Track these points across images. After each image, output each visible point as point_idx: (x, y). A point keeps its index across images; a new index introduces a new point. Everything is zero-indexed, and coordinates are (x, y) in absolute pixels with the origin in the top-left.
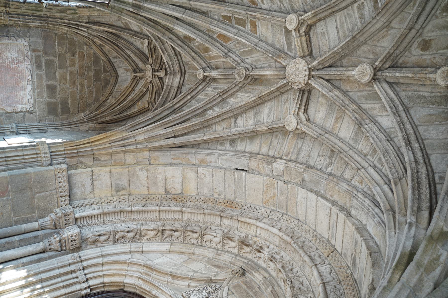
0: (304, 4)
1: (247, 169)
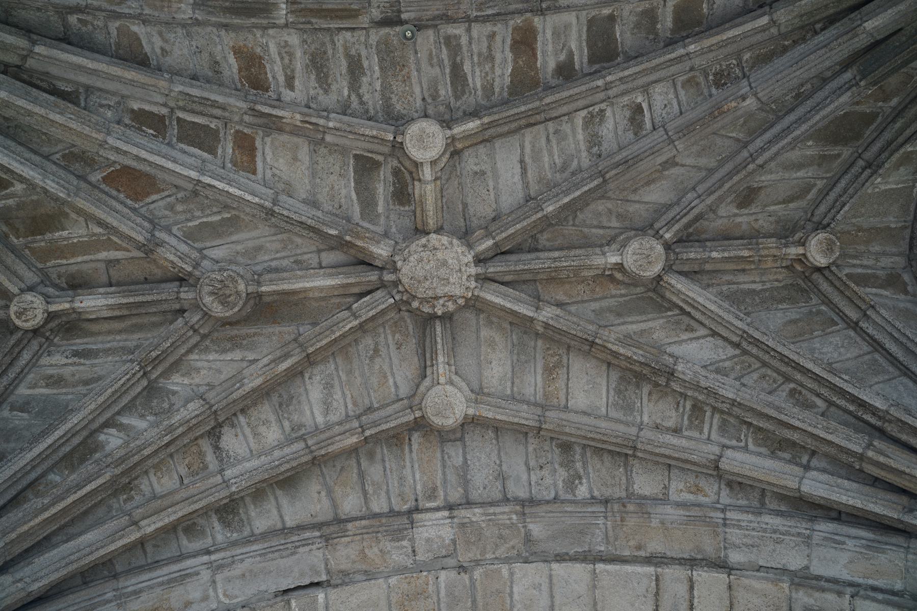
0: (429, 101)
1: (324, 578)
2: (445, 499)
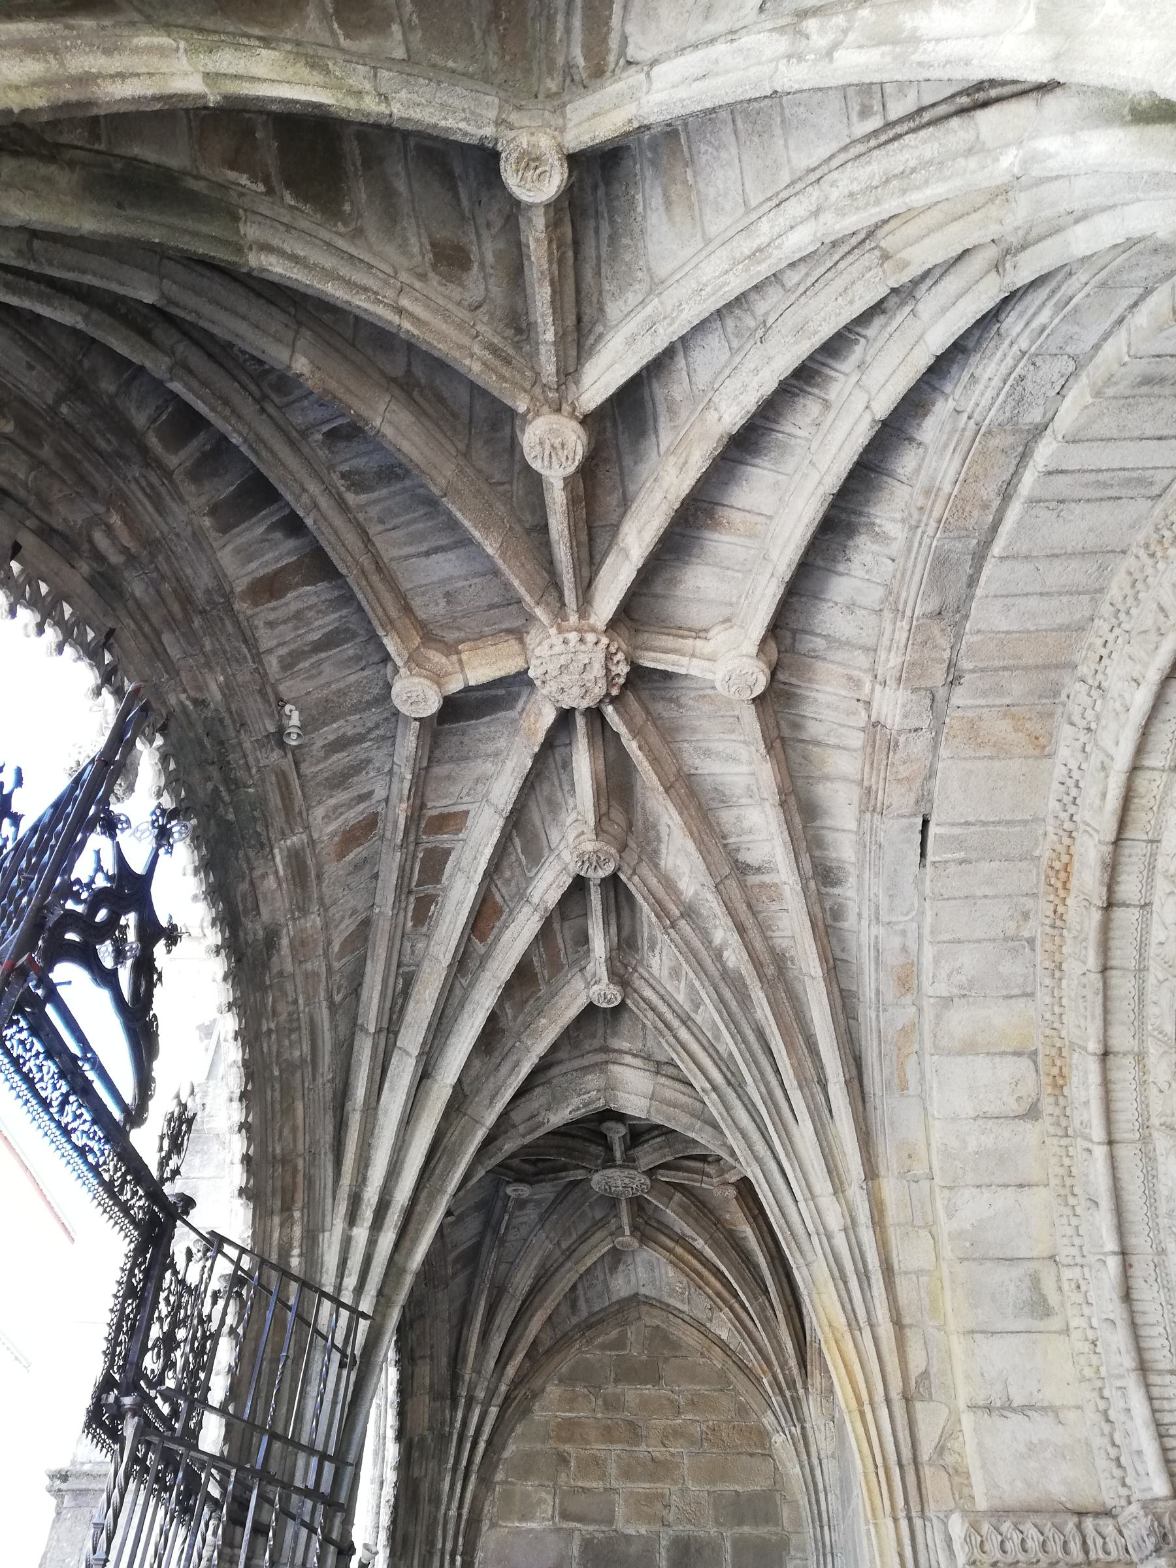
0: (363, 663)
1: (920, 820)
2: (865, 671)
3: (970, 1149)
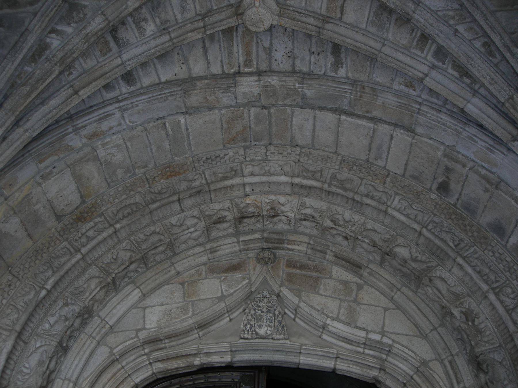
3: (35, 208)
